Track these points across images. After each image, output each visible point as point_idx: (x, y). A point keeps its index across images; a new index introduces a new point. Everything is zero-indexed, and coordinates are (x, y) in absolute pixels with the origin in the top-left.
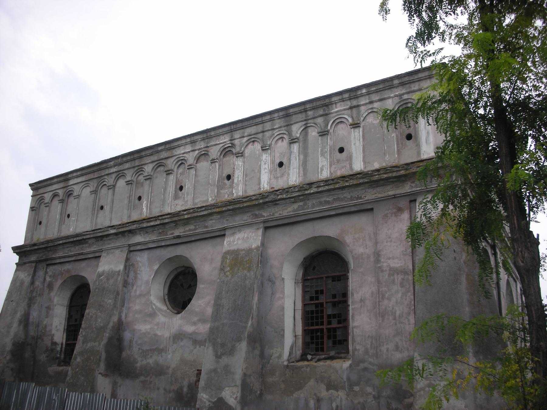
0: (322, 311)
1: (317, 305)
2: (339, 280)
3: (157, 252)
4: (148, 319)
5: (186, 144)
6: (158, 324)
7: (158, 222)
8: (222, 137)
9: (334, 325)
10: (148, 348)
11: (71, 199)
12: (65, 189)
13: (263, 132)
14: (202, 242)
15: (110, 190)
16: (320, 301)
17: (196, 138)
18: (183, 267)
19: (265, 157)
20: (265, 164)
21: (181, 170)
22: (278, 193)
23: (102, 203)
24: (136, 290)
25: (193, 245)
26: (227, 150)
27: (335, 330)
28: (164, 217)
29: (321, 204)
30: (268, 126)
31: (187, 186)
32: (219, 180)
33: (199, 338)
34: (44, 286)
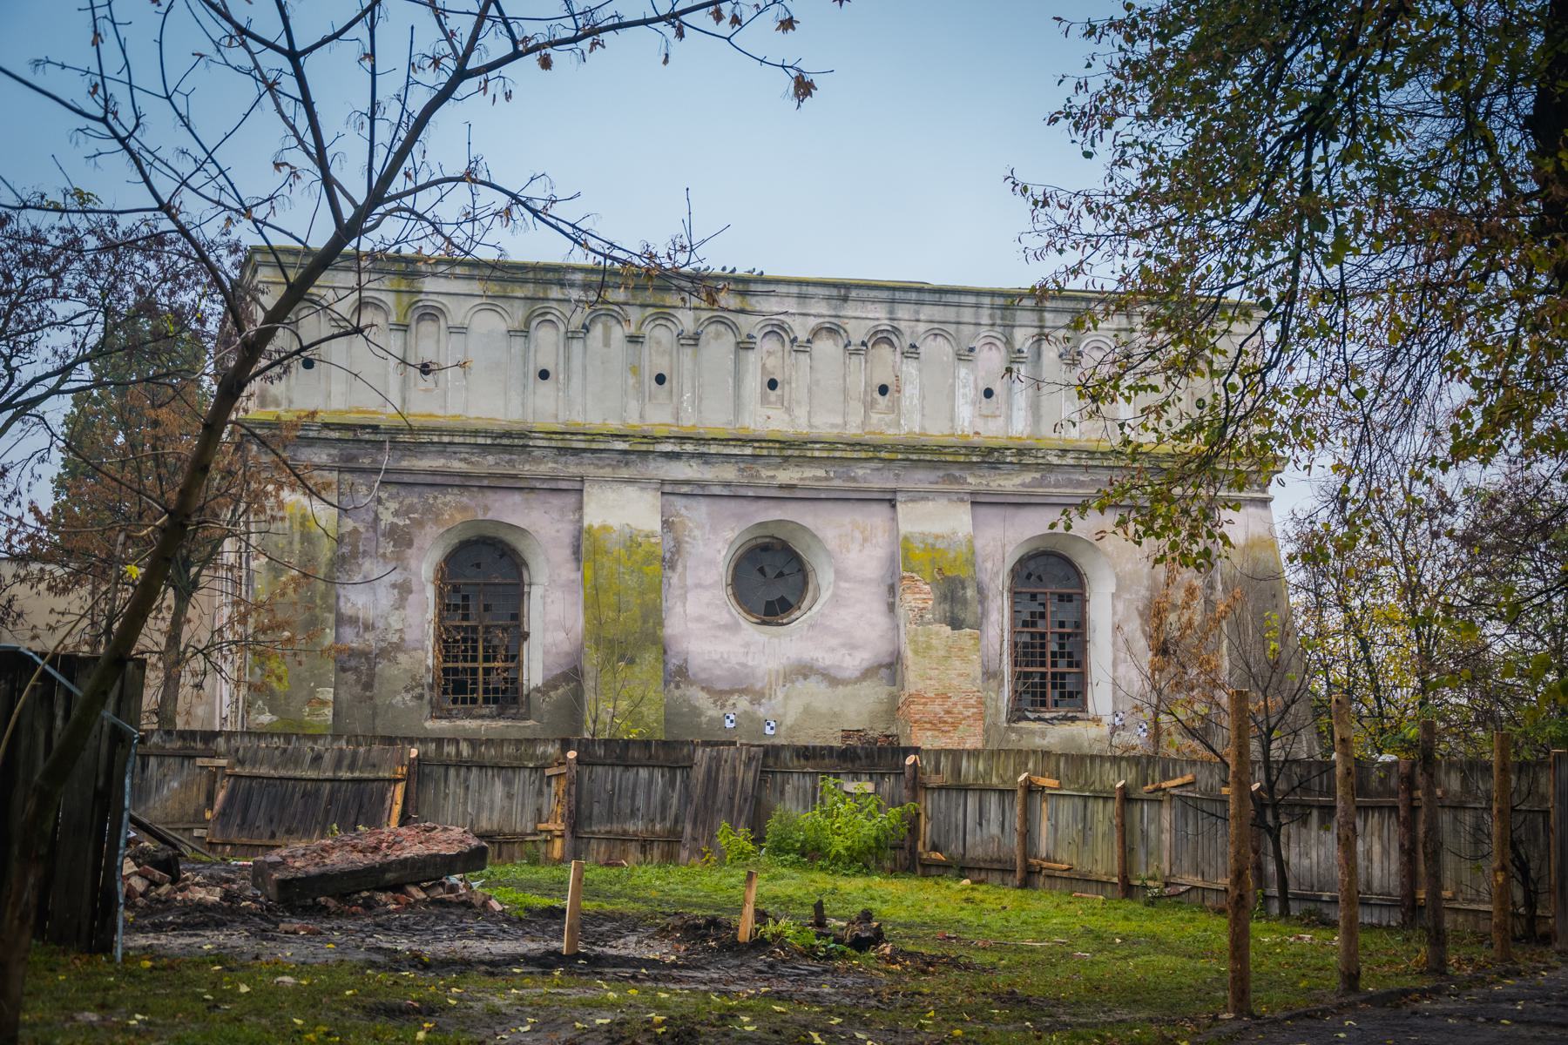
0: (1043, 646)
1: (1033, 635)
2: (1070, 600)
3: (733, 505)
4: (720, 633)
5: (788, 295)
6: (747, 645)
7: (748, 451)
8: (870, 306)
9: (1062, 667)
10: (727, 688)
11: (427, 327)
12: (406, 299)
13: (959, 323)
14: (840, 503)
15: (575, 341)
16: (1040, 629)
17: (811, 290)
18: (772, 537)
19: (963, 371)
20: (965, 386)
21: (771, 344)
22: (1008, 452)
23: (543, 365)
24: (683, 577)
25: (820, 505)
26: (879, 336)
27: (1063, 676)
28: (764, 444)
29: (1070, 483)
30: (967, 315)
31: (794, 385)
32: (866, 391)
33: (846, 674)
34: (375, 531)
